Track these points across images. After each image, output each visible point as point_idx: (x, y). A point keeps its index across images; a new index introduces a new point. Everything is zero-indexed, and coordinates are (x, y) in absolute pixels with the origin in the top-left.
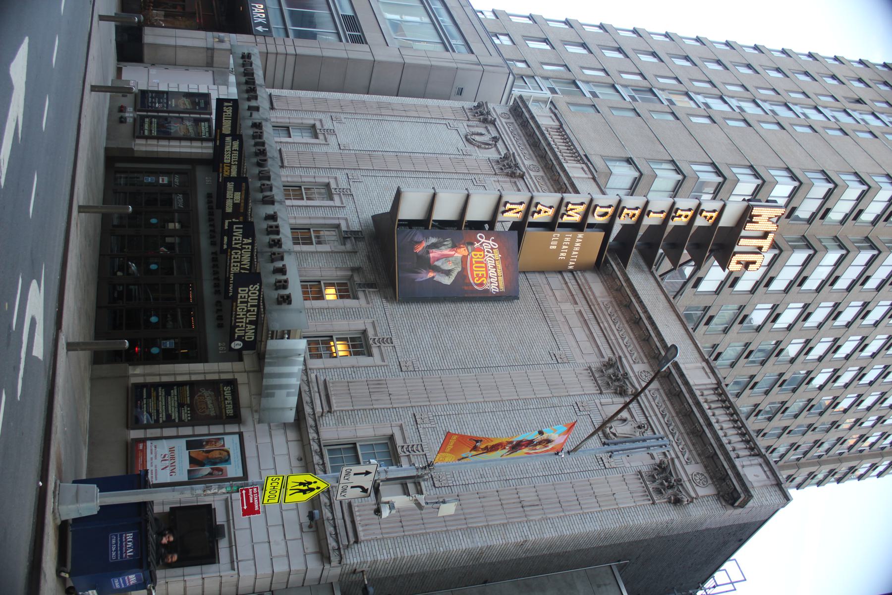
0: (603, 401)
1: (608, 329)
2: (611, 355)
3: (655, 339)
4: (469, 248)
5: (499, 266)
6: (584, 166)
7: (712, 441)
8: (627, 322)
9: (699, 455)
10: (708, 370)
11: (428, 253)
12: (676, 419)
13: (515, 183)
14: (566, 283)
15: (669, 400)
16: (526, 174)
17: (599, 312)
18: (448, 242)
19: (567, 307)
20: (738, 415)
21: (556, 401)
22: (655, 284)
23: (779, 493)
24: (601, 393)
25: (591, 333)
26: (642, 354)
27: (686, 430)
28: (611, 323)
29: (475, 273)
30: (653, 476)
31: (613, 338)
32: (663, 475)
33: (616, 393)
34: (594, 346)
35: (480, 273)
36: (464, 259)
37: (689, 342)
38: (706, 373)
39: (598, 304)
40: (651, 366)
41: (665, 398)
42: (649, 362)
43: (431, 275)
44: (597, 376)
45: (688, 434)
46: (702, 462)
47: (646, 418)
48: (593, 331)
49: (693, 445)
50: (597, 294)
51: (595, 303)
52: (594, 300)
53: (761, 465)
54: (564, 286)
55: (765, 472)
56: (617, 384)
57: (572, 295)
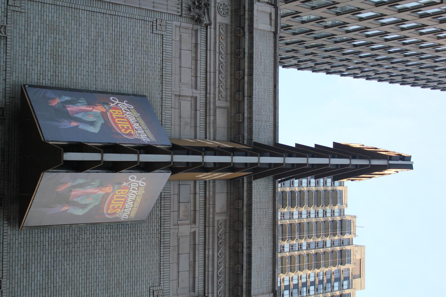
1: (211, 258)
3: (244, 280)
4: (116, 187)
5: (139, 200)
6: (273, 10)
8: (230, 248)
11: (71, 191)
13: (196, 31)
14: (195, 194)
16: (212, 26)
17: (211, 236)
18: (97, 183)
19: (185, 230)
22: (271, 195)
25: (195, 261)
26: (227, 287)
29: (112, 205)
31: (210, 269)
34: (191, 277)
35: (117, 206)
36: (107, 194)
37: (270, 268)
39: (214, 226)
43: (66, 208)
48: (197, 259)
50: (218, 210)
51: (211, 224)
52: (211, 220)
54: (192, 196)
57: (195, 211)
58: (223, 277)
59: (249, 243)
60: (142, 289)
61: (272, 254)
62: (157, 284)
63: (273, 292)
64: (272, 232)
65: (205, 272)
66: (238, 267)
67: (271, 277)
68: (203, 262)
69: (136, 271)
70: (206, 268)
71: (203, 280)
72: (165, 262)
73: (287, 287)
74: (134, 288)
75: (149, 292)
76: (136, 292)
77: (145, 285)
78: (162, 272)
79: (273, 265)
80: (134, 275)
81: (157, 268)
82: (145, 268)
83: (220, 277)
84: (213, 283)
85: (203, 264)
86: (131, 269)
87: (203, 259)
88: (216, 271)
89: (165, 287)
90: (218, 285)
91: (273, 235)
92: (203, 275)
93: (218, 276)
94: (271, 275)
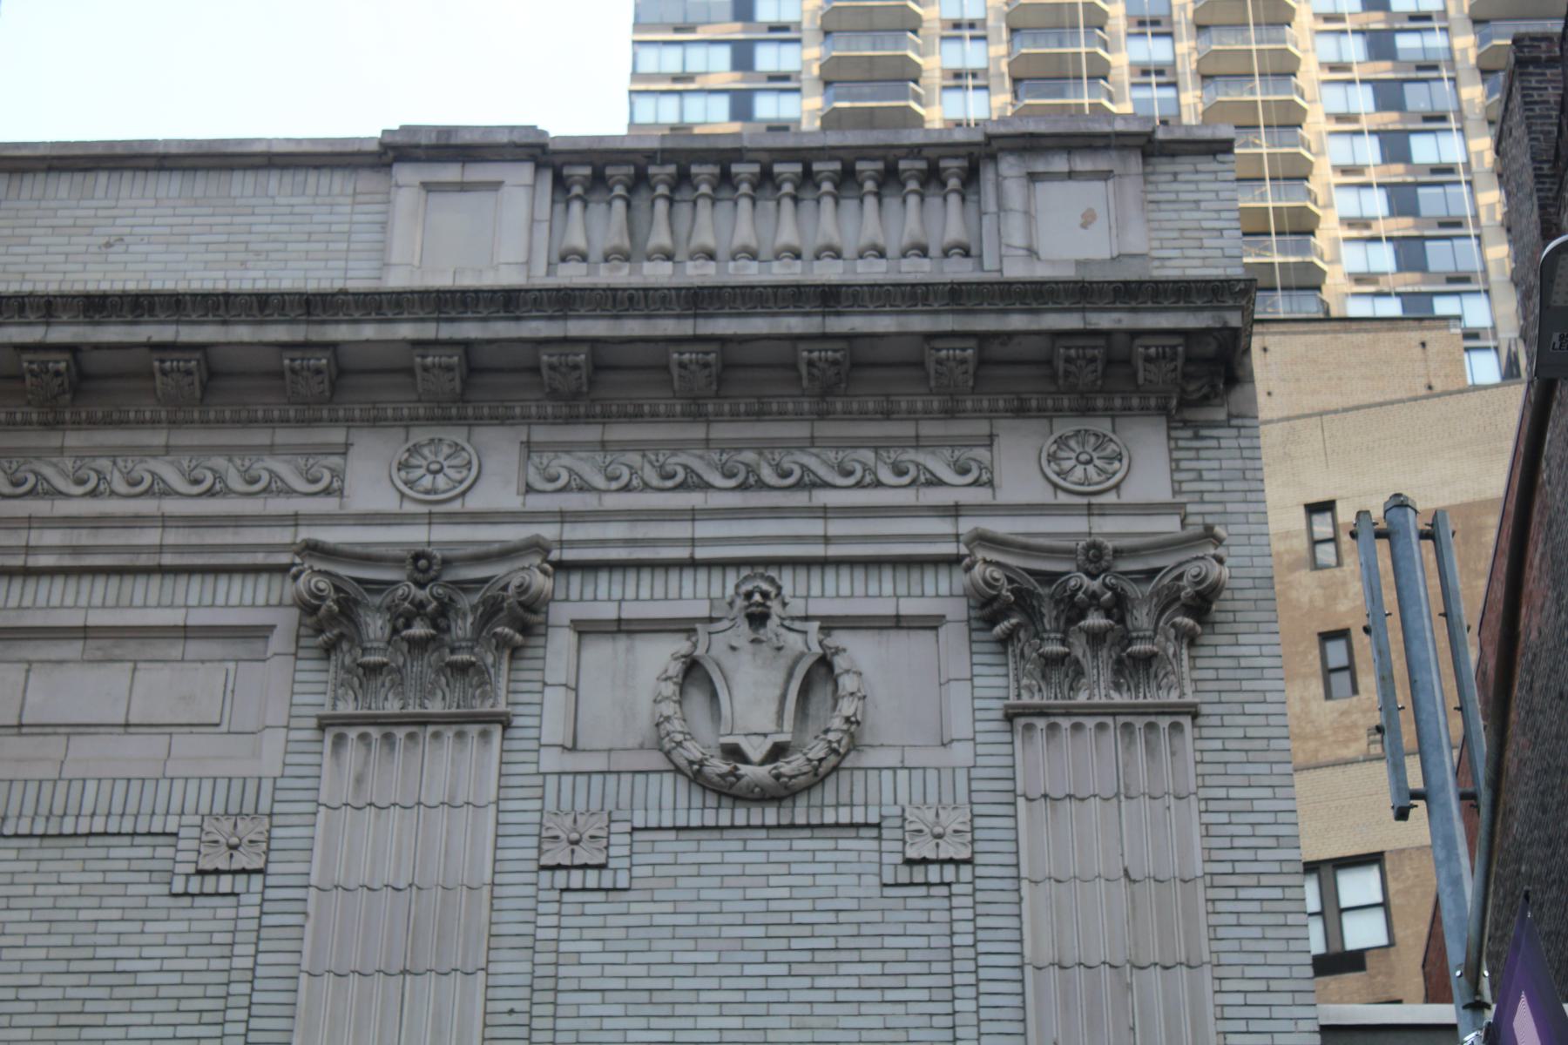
0: (554, 728)
1: (84, 538)
2: (288, 589)
3: (243, 333)
7: (920, 323)
9: (950, 414)
10: (450, 173)
12: (721, 431)
15: (606, 418)
20: (739, 154)
21: (512, 966)
23: (1184, 165)
24: (505, 722)
26: (284, 436)
27: (798, 416)
28: (40, 507)
30: (1051, 662)
31: (151, 537)
32: (1049, 612)
33: (516, 652)
34: (175, 650)
37: (242, 185)
38: (463, 187)
40: (375, 422)
41: (591, 433)
42: (350, 422)
44: (393, 706)
45: (823, 415)
46: (992, 414)
47: (693, 564)
49: (887, 415)
53: (1033, 177)
55: (1071, 175)
56: (462, 628)
58: (220, 462)
59: (21, 309)
60: (172, 939)
61: (164, 176)
62: (160, 852)
63: (389, 166)
64: (28, 180)
65: (163, 570)
66: (164, 373)
67: (300, 176)
68: (100, 582)
69: (49, 980)
70: (144, 560)
71: (210, 579)
72: (44, 809)
73: (741, 104)
74: (150, 992)
75: (199, 901)
76: (176, 978)
77: (150, 927)
78: (98, 826)
79: (231, 168)
80: (71, 993)
81: (69, 853)
82: (44, 927)
83: (219, 476)
84: (237, 521)
85: (114, 581)
86: (30, 1007)
87: (86, 582)
88: (172, 506)
89: (190, 805)
90: (264, 490)
91: (50, 169)
92: (182, 581)
93: (210, 493)
94: (288, 177)
